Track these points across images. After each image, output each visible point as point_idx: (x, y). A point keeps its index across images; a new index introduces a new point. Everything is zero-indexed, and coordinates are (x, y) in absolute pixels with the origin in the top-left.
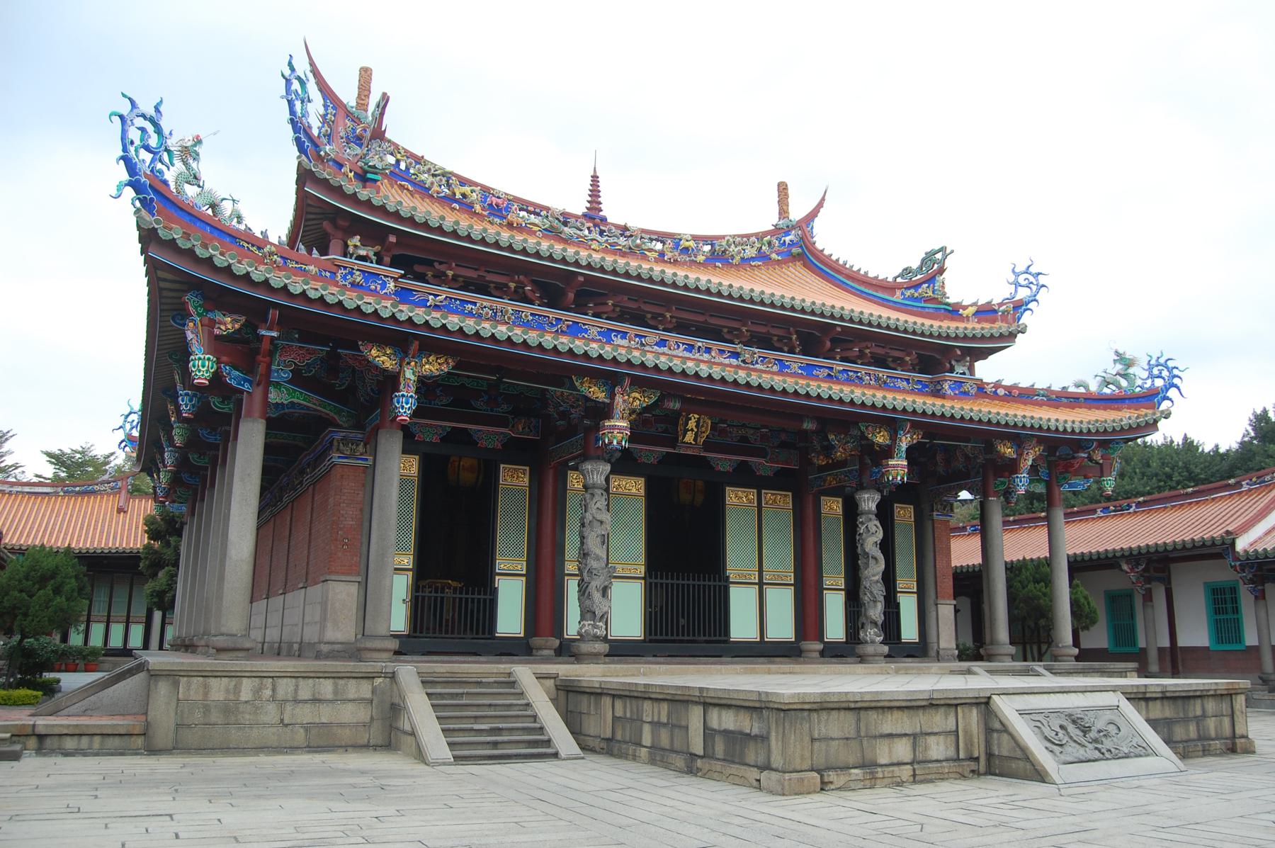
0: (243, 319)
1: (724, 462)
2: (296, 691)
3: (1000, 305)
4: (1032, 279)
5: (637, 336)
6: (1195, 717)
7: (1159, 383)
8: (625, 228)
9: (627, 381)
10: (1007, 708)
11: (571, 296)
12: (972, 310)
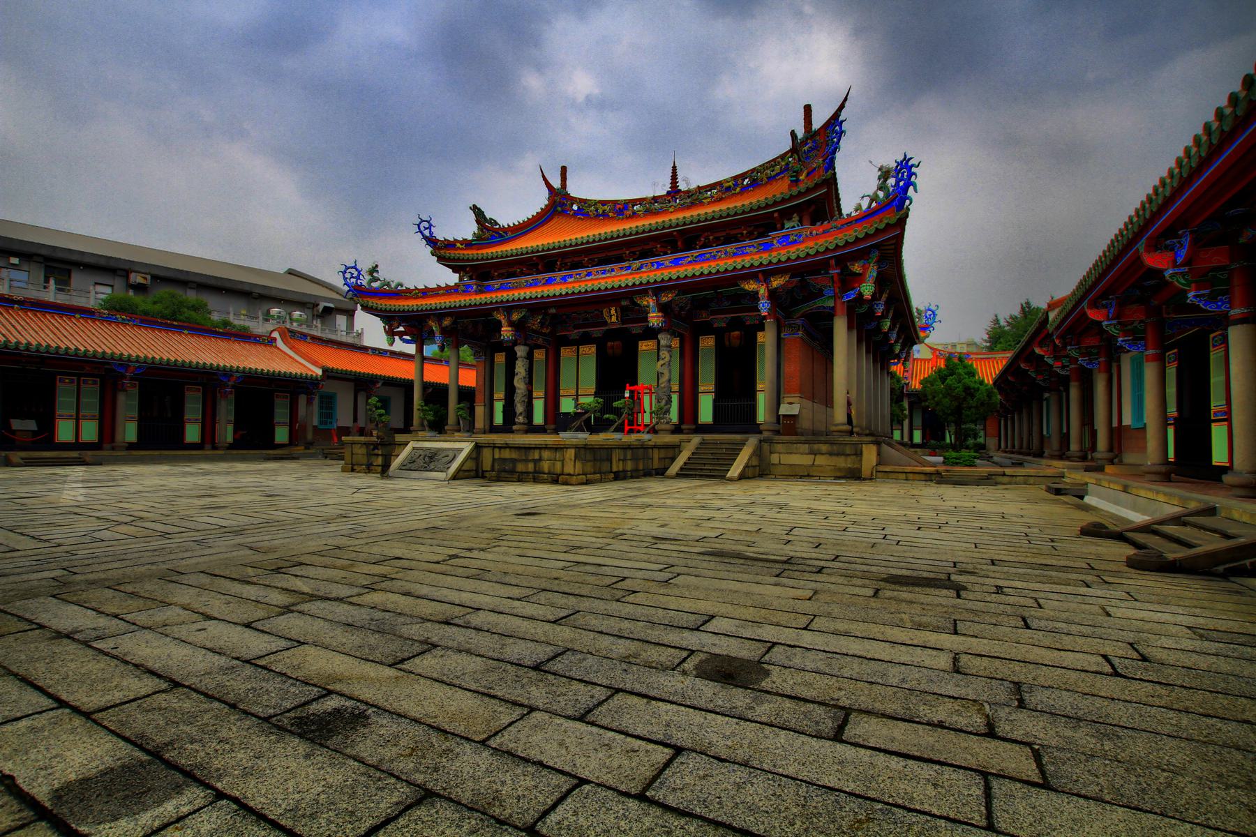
8: (688, 192)
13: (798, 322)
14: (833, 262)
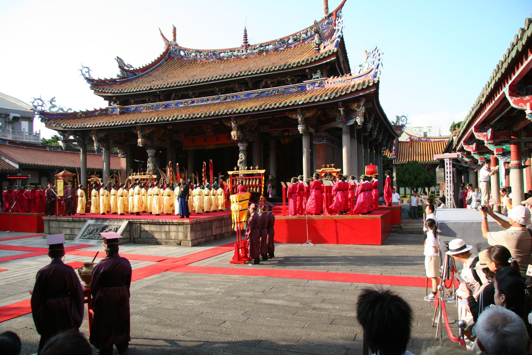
13: (323, 134)
14: (340, 104)
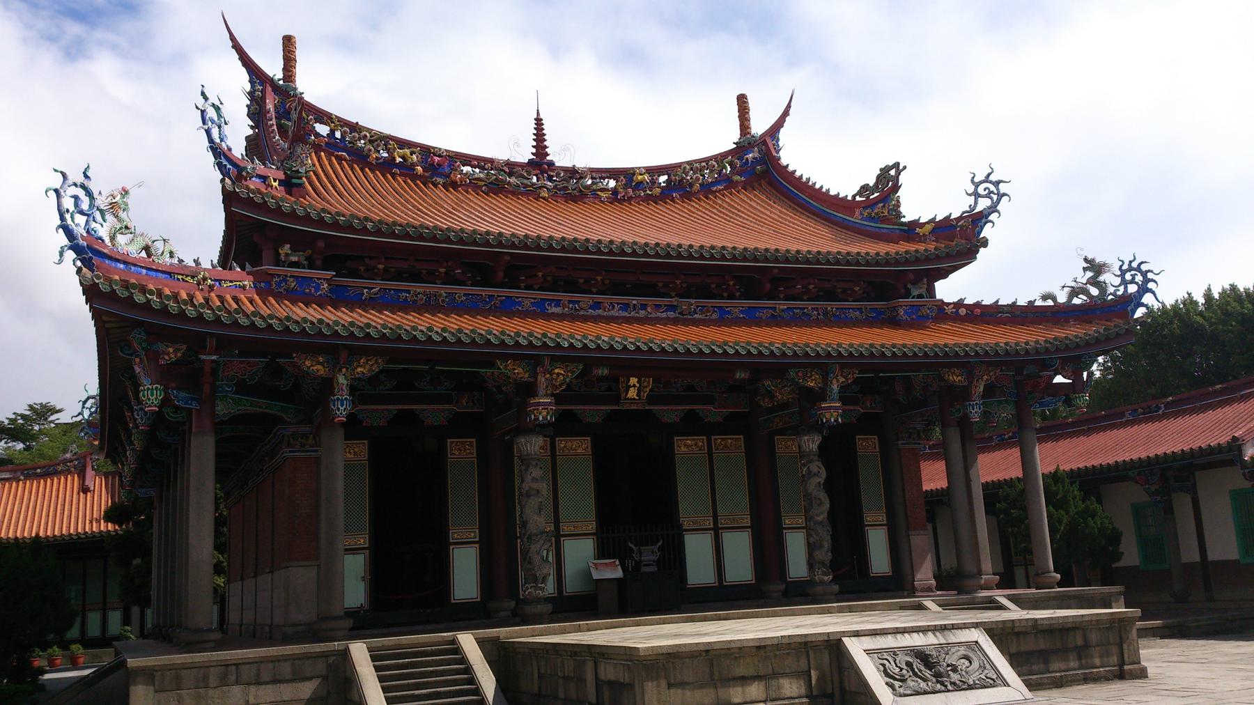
0: (185, 347)
1: (670, 413)
2: (258, 674)
3: (960, 218)
4: (992, 188)
5: (570, 302)
6: (1076, 647)
7: (1132, 289)
9: (547, 362)
10: (855, 648)
11: (501, 274)
12: (929, 227)
